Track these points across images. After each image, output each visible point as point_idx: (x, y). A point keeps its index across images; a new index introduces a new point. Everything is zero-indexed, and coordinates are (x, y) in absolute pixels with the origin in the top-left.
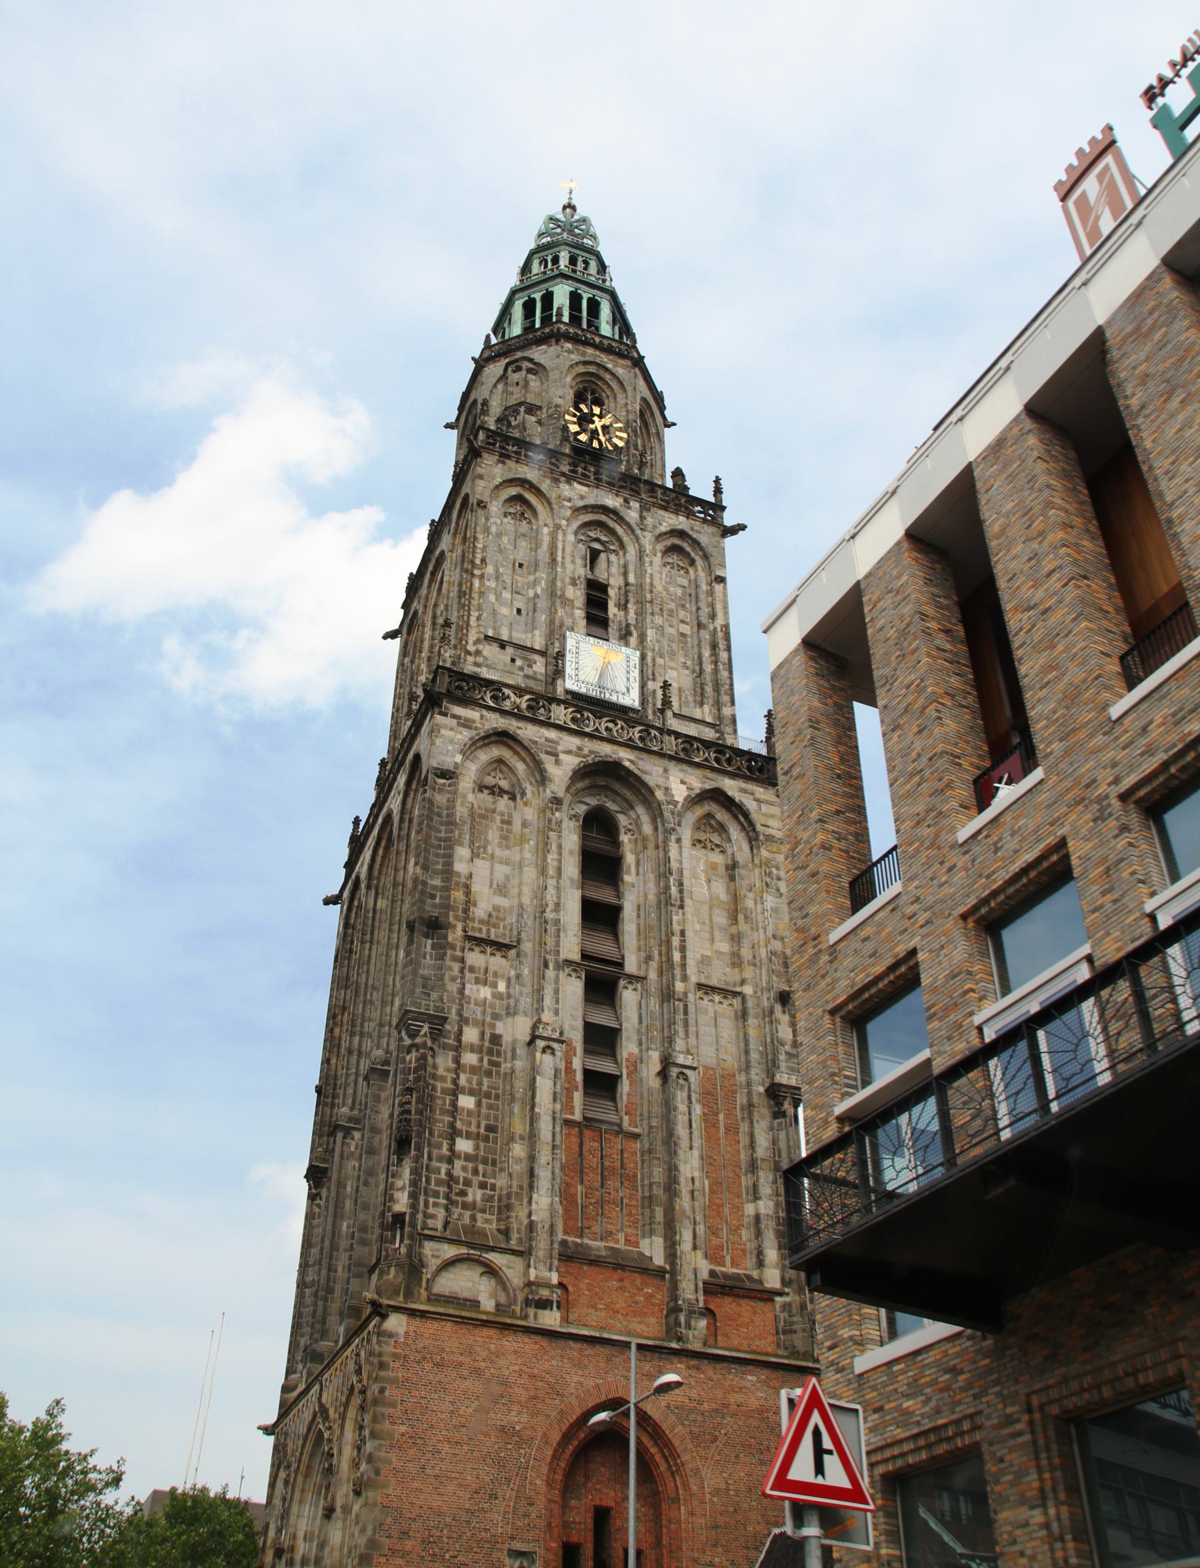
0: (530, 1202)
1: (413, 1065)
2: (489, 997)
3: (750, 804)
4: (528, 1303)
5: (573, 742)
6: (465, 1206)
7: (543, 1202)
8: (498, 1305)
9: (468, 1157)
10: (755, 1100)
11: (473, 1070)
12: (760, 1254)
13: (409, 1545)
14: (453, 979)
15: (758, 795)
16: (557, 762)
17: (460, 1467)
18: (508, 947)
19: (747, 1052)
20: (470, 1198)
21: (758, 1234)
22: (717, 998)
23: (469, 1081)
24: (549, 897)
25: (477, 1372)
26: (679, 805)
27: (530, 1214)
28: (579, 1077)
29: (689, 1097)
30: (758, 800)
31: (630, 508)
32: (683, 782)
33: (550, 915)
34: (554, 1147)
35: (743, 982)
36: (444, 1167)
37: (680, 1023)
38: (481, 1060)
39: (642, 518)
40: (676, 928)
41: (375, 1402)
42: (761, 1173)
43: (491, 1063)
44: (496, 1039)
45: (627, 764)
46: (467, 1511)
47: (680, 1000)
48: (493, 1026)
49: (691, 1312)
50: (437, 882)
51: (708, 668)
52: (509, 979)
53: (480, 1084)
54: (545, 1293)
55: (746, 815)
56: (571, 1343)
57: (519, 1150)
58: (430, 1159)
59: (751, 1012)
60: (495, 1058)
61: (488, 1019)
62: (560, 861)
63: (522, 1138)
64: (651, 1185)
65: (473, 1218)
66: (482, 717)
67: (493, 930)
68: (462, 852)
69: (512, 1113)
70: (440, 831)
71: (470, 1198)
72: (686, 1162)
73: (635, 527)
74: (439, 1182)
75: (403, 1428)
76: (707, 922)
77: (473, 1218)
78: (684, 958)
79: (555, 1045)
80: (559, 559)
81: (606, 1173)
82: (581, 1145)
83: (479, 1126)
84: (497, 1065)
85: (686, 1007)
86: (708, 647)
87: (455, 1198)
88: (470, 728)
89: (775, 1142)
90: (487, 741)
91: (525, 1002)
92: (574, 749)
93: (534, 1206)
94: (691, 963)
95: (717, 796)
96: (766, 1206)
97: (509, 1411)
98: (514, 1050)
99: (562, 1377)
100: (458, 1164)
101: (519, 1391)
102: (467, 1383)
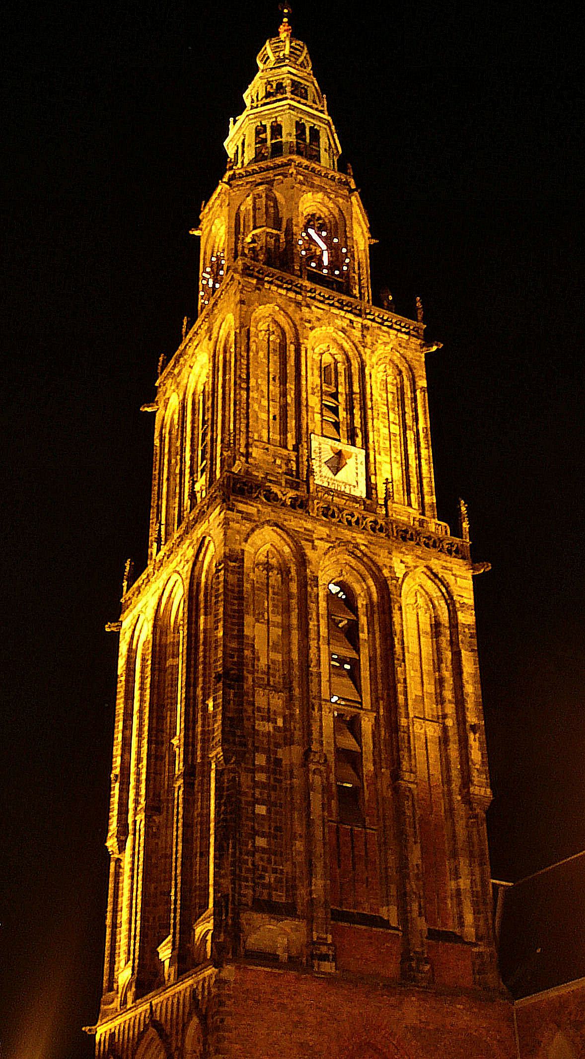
0: (310, 884)
1: (226, 785)
2: (271, 729)
3: (450, 579)
4: (312, 956)
5: (323, 531)
6: (263, 885)
7: (319, 883)
8: (289, 957)
9: (264, 850)
10: (456, 806)
11: (264, 786)
12: (461, 917)
14: (249, 719)
16: (314, 548)
19: (448, 770)
20: (267, 881)
21: (460, 904)
23: (261, 794)
24: (312, 656)
25: (282, 1007)
26: (400, 580)
27: (311, 893)
29: (413, 805)
32: (402, 562)
33: (313, 669)
34: (324, 844)
36: (250, 859)
37: (406, 750)
38: (269, 778)
39: (364, 336)
40: (400, 677)
41: (217, 1029)
42: (461, 859)
43: (276, 780)
44: (278, 762)
47: (404, 732)
48: (276, 753)
49: (419, 961)
50: (234, 645)
51: (413, 462)
52: (284, 717)
53: (269, 796)
54: (324, 949)
55: (447, 587)
57: (299, 845)
58: (241, 853)
59: (452, 739)
60: (278, 777)
61: (272, 747)
63: (301, 836)
64: (386, 868)
65: (270, 895)
66: (258, 510)
67: (271, 679)
68: (249, 619)
69: (292, 819)
70: (234, 604)
71: (267, 881)
74: (248, 870)
75: (238, 1046)
76: (419, 668)
77: (270, 895)
78: (406, 700)
79: (322, 768)
80: (303, 373)
82: (338, 840)
83: (270, 828)
84: (280, 781)
85: (409, 737)
86: (413, 445)
87: (257, 881)
88: (250, 520)
89: (470, 837)
91: (297, 734)
92: (325, 536)
93: (313, 888)
94: (410, 702)
96: (464, 883)
98: (291, 772)
100: (257, 856)
101: (310, 1019)
102: (277, 1014)
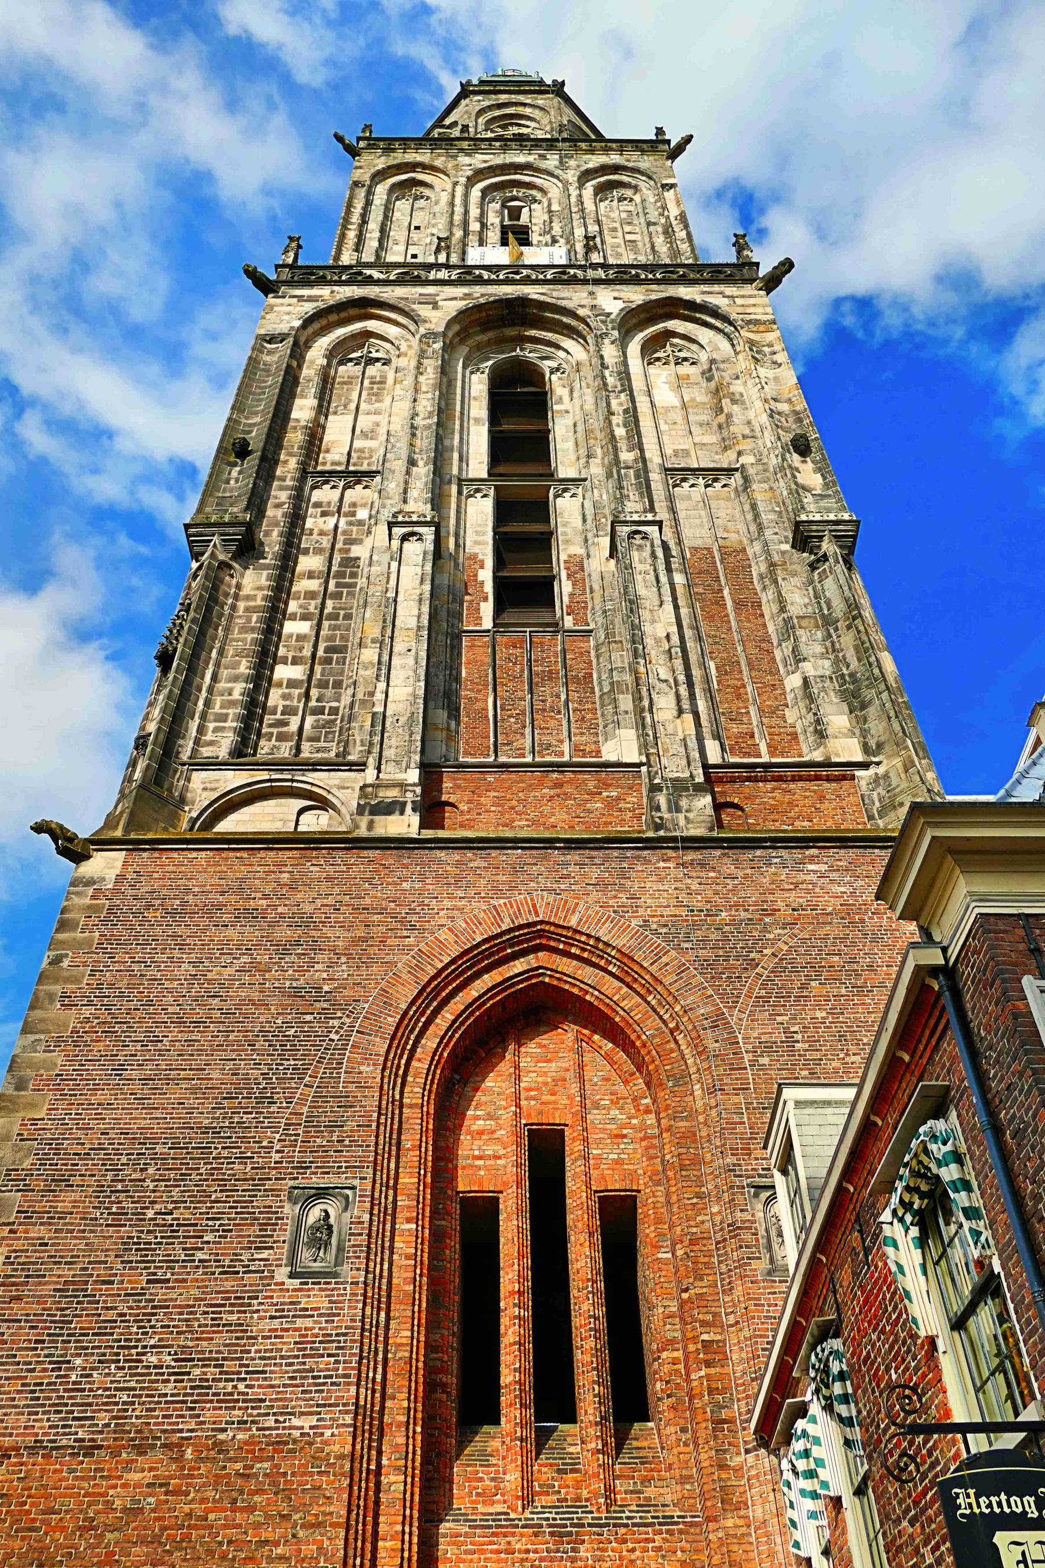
13: (66, 1201)
17: (200, 1060)
18: (371, 474)
45: (535, 297)
46: (206, 1130)
55: (715, 312)
56: (442, 854)
72: (653, 621)
81: (535, 680)
90: (344, 315)
97: (312, 963)
99: (422, 904)
102: (230, 932)
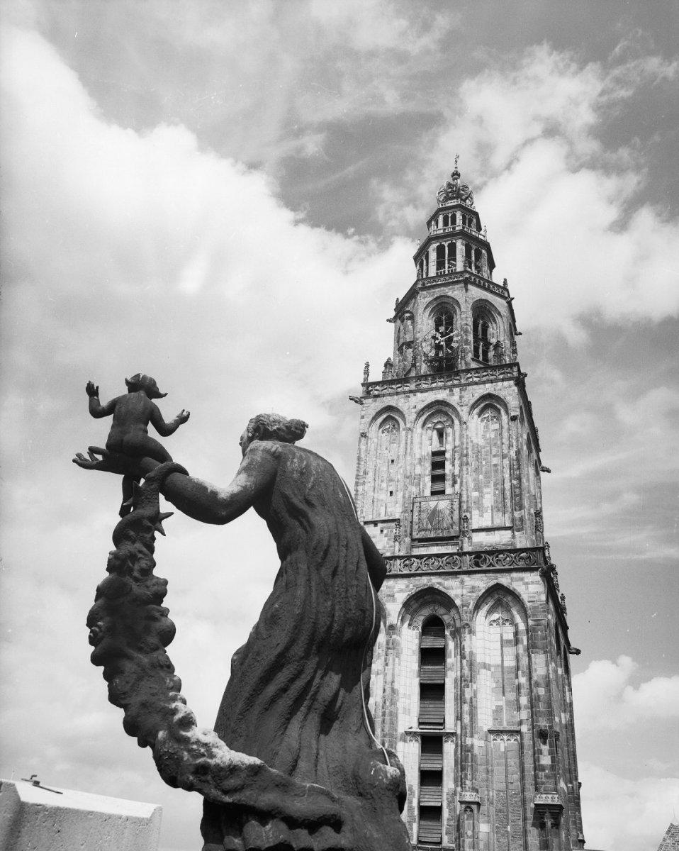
5: (402, 583)
15: (526, 580)
22: (505, 737)
28: (416, 812)
30: (527, 584)
31: (453, 395)
35: (521, 723)
45: (437, 586)
62: (394, 669)
73: (456, 406)
95: (498, 588)
